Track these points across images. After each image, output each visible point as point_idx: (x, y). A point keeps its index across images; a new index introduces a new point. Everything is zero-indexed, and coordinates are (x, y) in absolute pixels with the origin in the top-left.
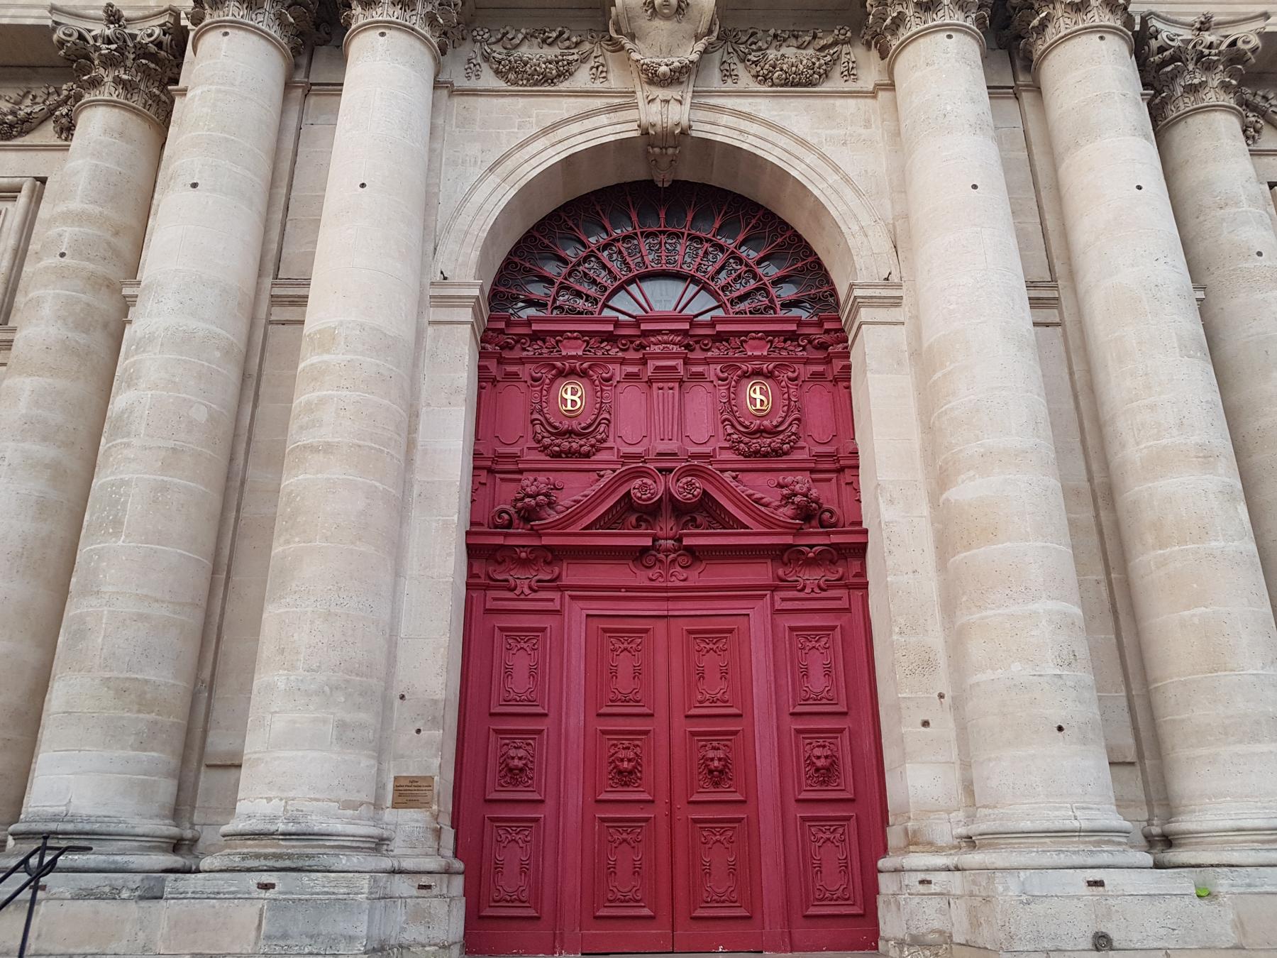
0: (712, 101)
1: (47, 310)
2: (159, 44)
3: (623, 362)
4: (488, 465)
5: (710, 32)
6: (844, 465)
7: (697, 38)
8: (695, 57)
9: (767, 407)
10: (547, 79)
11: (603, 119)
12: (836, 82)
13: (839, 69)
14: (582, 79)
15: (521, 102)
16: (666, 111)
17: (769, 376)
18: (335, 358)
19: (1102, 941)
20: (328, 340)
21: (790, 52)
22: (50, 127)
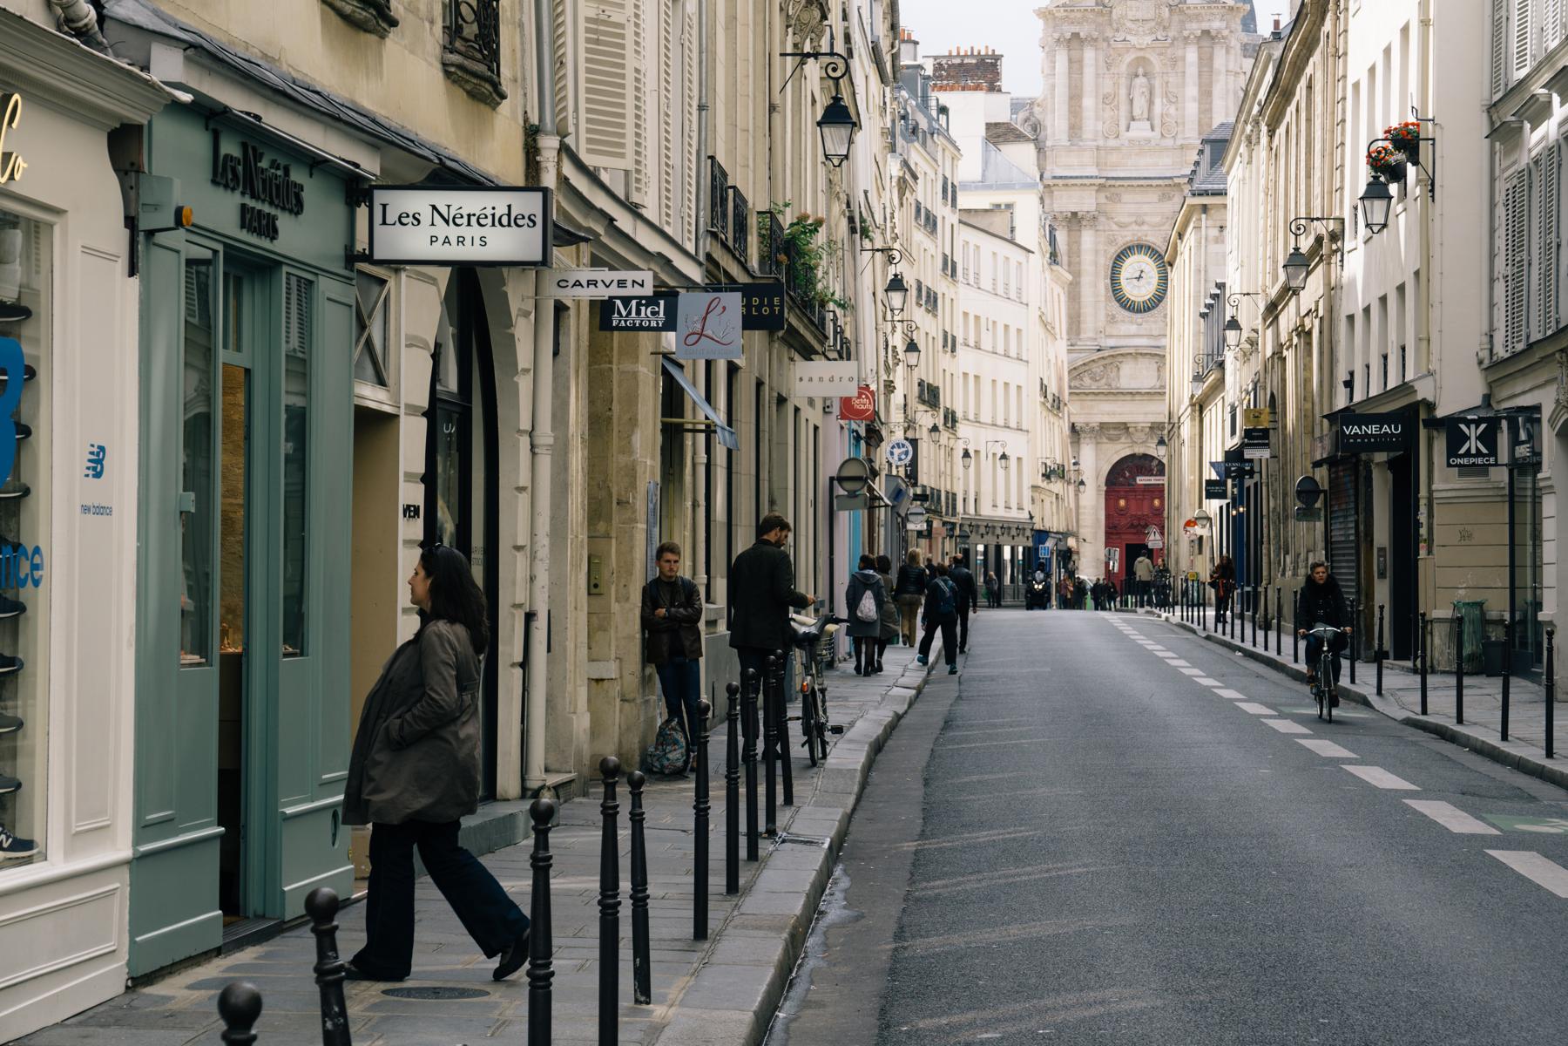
4: (1108, 517)
16: (1139, 450)
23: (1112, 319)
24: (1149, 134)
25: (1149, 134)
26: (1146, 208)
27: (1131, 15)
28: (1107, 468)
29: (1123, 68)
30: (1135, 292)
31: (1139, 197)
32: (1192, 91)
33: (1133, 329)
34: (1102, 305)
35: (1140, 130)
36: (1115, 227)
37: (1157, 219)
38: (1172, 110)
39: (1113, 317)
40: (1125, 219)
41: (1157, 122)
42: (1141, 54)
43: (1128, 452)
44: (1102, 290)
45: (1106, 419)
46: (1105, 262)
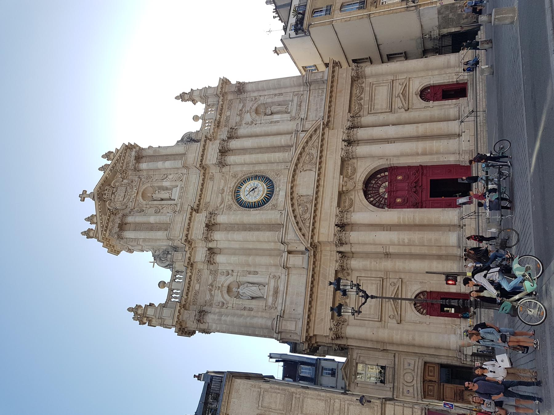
1: (386, 263)
6: (410, 168)
12: (355, 165)
14: (352, 197)
16: (360, 186)
18: (402, 216)
19: (469, 141)
20: (399, 218)
21: (349, 171)
23: (274, 207)
24: (178, 188)
25: (178, 188)
26: (215, 188)
27: (121, 199)
28: (371, 207)
30: (261, 193)
31: (209, 193)
33: (282, 193)
35: (176, 194)
36: (222, 206)
37: (223, 181)
38: (170, 177)
40: (219, 200)
41: (174, 184)
42: (140, 194)
43: (361, 194)
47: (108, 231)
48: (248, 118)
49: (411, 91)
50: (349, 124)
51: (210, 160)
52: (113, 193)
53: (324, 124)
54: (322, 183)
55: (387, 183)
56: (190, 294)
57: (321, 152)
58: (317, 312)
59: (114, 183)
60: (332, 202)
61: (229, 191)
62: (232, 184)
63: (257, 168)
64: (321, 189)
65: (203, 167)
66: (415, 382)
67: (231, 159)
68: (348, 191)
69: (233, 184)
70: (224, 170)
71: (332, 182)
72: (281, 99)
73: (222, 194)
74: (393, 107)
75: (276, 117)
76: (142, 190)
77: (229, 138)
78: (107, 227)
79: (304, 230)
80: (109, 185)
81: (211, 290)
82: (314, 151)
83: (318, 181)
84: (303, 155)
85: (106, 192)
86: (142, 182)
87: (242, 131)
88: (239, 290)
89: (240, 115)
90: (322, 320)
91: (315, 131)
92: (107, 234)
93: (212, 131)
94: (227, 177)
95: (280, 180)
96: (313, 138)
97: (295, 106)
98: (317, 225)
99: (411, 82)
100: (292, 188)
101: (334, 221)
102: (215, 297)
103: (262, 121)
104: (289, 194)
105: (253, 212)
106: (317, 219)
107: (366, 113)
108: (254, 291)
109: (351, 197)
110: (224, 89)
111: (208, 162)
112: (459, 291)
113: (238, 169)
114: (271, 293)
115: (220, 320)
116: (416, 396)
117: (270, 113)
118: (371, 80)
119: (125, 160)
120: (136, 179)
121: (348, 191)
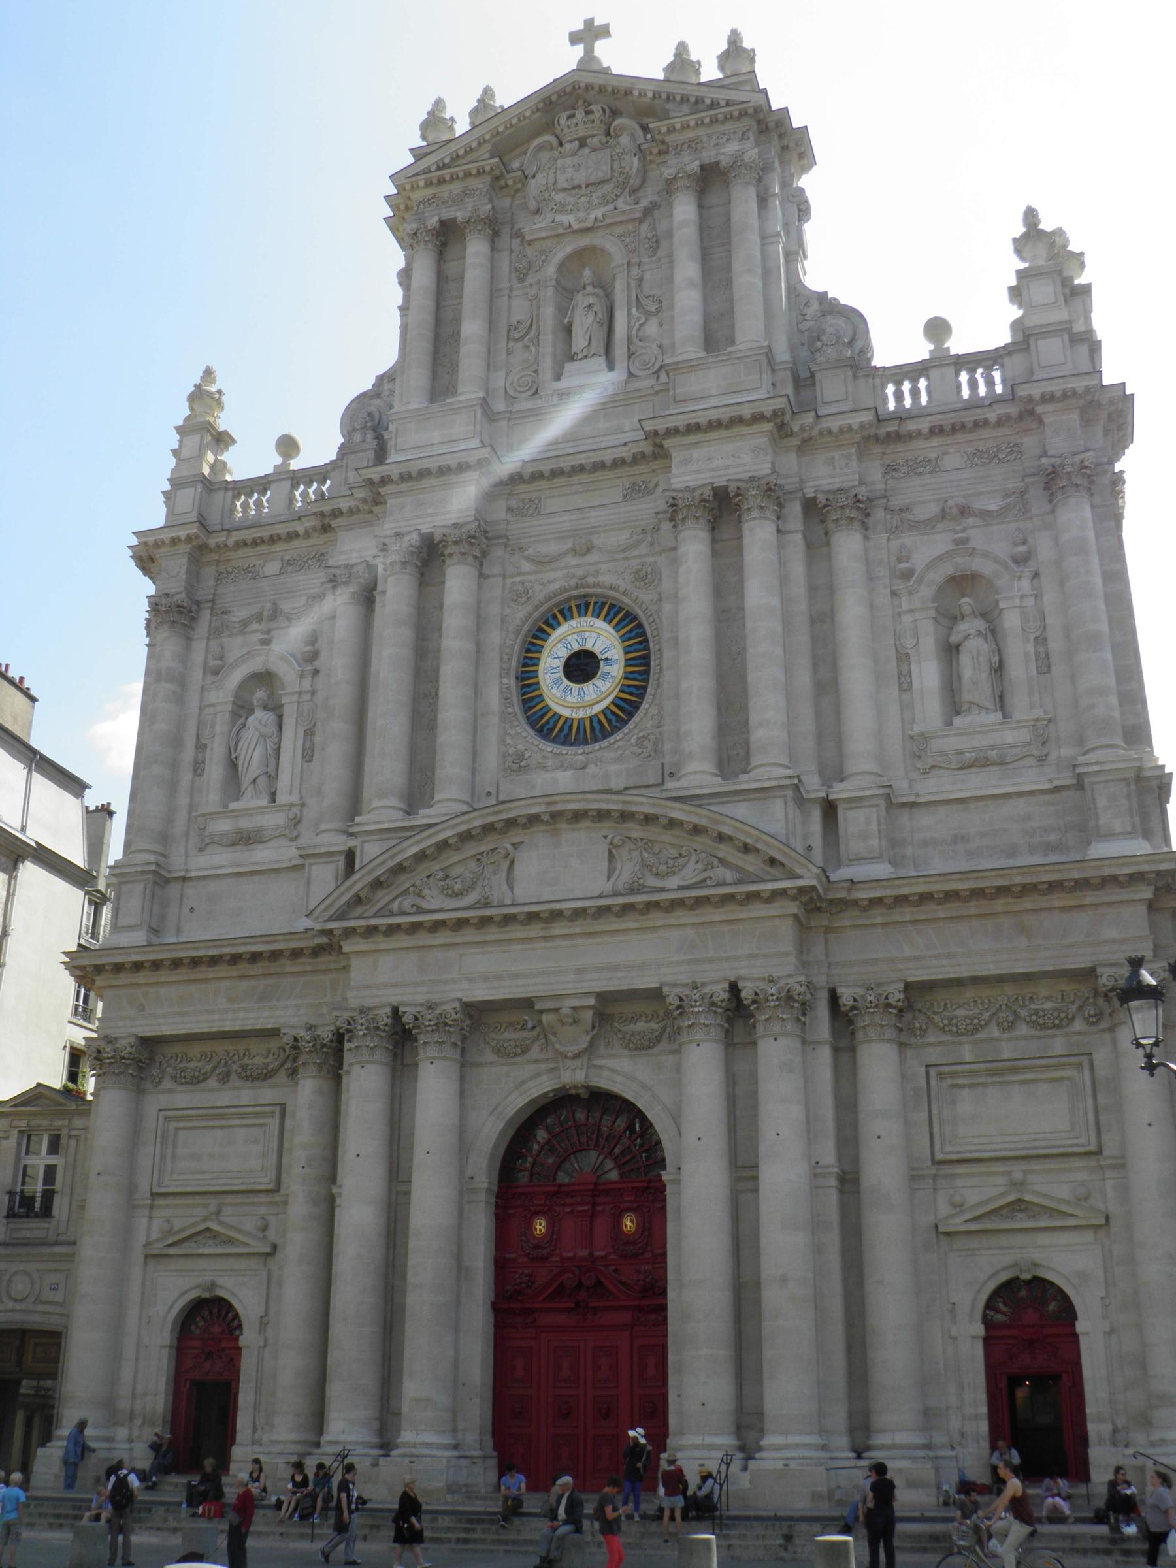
0: (599, 1062)
2: (331, 1041)
3: (564, 1205)
5: (593, 1027)
7: (587, 1033)
8: (585, 1045)
9: (633, 1229)
10: (516, 1055)
11: (545, 1077)
13: (666, 1035)
14: (535, 1053)
15: (505, 1068)
16: (574, 1076)
17: (634, 1210)
21: (641, 1026)
22: (282, 1072)
23: (517, 765)
27: (562, 182)
28: (490, 1130)
29: (551, 270)
30: (572, 699)
32: (687, 269)
33: (564, 780)
34: (492, 735)
36: (526, 566)
37: (623, 537)
39: (520, 757)
40: (554, 548)
42: (585, 241)
43: (542, 1085)
44: (493, 695)
45: (481, 993)
46: (502, 642)
47: (430, 191)
48: (927, 549)
49: (1044, 1239)
50: (846, 996)
51: (687, 462)
52: (582, 142)
53: (802, 890)
54: (558, 929)
55: (614, 1175)
56: (248, 551)
57: (679, 904)
58: (163, 991)
59: (622, 129)
60: (485, 979)
61: (580, 572)
62: (610, 577)
63: (667, 654)
64: (535, 930)
65: (658, 448)
66: (10, 1305)
67: (694, 546)
68: (545, 1035)
69: (606, 579)
70: (666, 526)
71: (565, 971)
72: (1019, 669)
73: (574, 551)
74: (961, 1169)
75: (928, 674)
76: (598, 242)
77: (811, 508)
78: (442, 181)
79: (383, 897)
80: (615, 113)
81: (259, 617)
82: (690, 873)
83: (556, 915)
84: (676, 832)
85: (580, 114)
86: (631, 227)
87: (848, 546)
88: (259, 714)
89: (943, 515)
90: (141, 1008)
91: (772, 861)
92: (417, 195)
93: (834, 424)
94: (643, 549)
95: (618, 760)
96: (750, 857)
97: (979, 741)
98: (402, 941)
99: (1089, 1236)
100: (534, 819)
101: (411, 999)
102: (238, 640)
103: (907, 619)
104: (505, 816)
105: (497, 690)
106: (423, 939)
107: (933, 1055)
108: (253, 759)
109: (535, 1049)
110: (1050, 407)
111: (677, 456)
112: (239, 1437)
113: (666, 585)
114: (245, 824)
115: (158, 680)
116: (40, 1308)
117: (954, 638)
118: (1101, 1056)
119: (701, 132)
120: (644, 203)
121: (545, 1035)
